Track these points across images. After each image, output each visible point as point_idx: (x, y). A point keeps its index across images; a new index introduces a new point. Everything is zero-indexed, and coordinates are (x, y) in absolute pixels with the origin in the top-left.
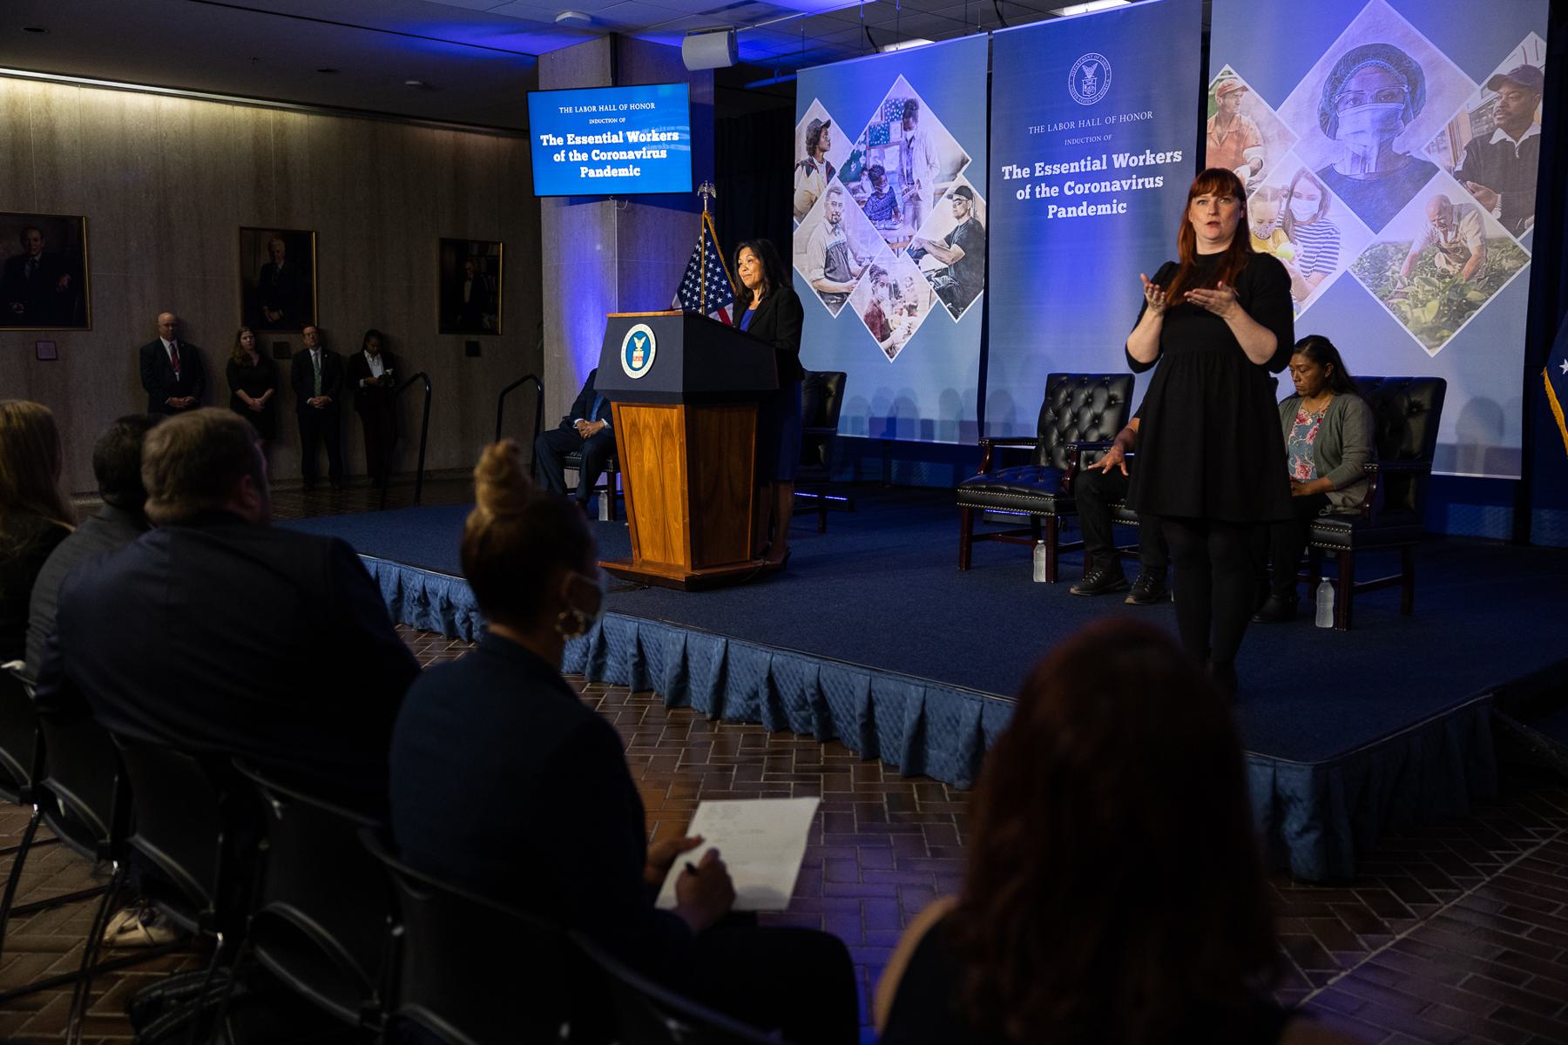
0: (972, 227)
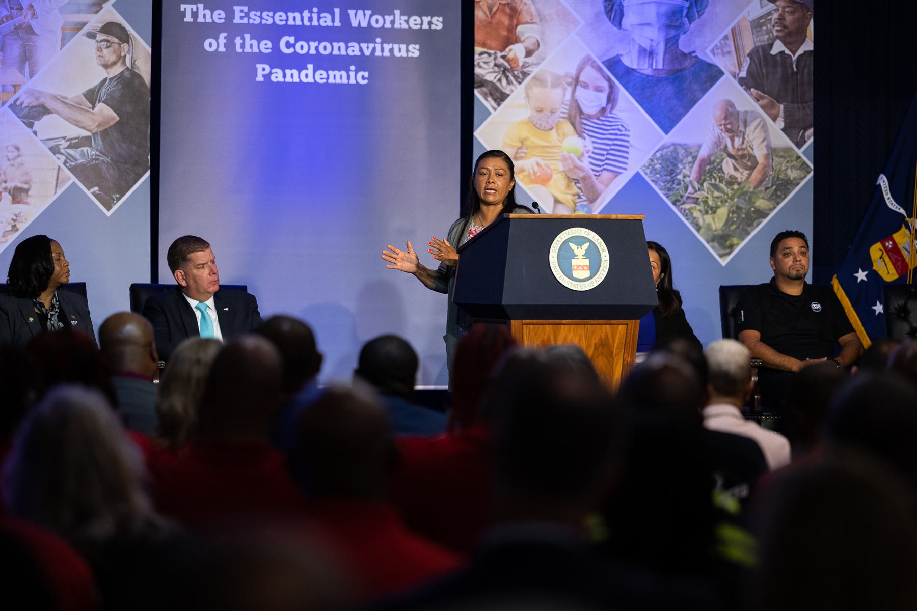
0: (129, 80)
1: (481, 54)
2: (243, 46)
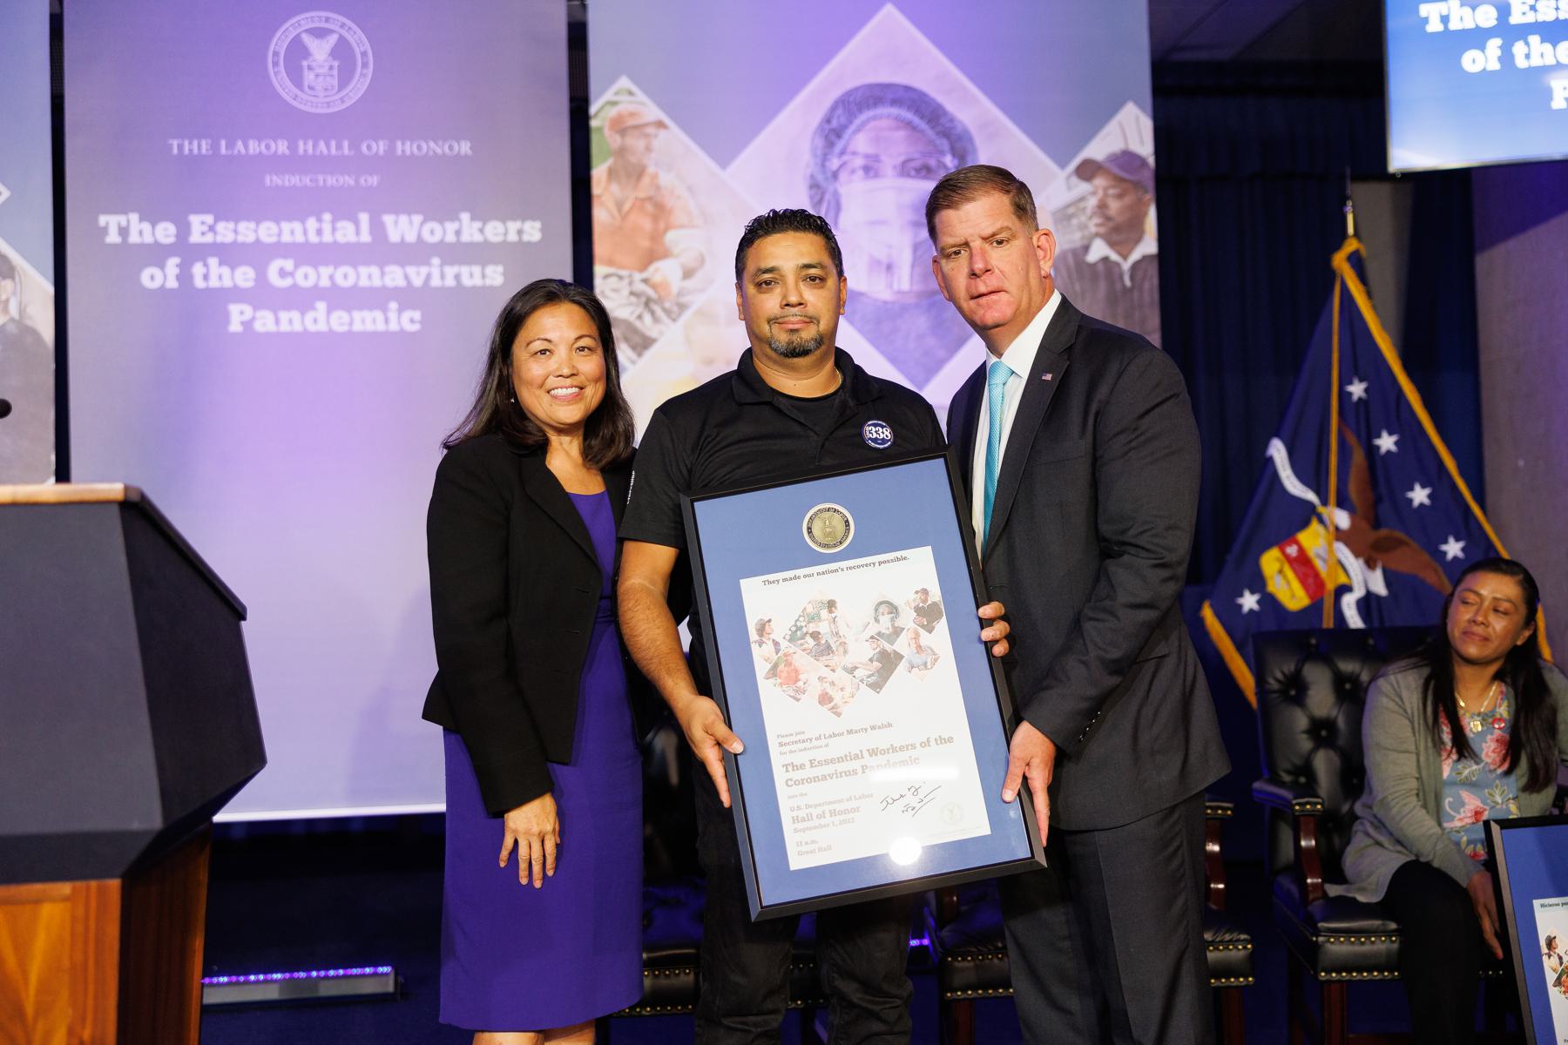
1: (606, 277)
2: (206, 277)
